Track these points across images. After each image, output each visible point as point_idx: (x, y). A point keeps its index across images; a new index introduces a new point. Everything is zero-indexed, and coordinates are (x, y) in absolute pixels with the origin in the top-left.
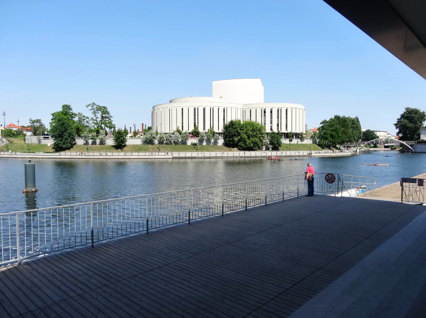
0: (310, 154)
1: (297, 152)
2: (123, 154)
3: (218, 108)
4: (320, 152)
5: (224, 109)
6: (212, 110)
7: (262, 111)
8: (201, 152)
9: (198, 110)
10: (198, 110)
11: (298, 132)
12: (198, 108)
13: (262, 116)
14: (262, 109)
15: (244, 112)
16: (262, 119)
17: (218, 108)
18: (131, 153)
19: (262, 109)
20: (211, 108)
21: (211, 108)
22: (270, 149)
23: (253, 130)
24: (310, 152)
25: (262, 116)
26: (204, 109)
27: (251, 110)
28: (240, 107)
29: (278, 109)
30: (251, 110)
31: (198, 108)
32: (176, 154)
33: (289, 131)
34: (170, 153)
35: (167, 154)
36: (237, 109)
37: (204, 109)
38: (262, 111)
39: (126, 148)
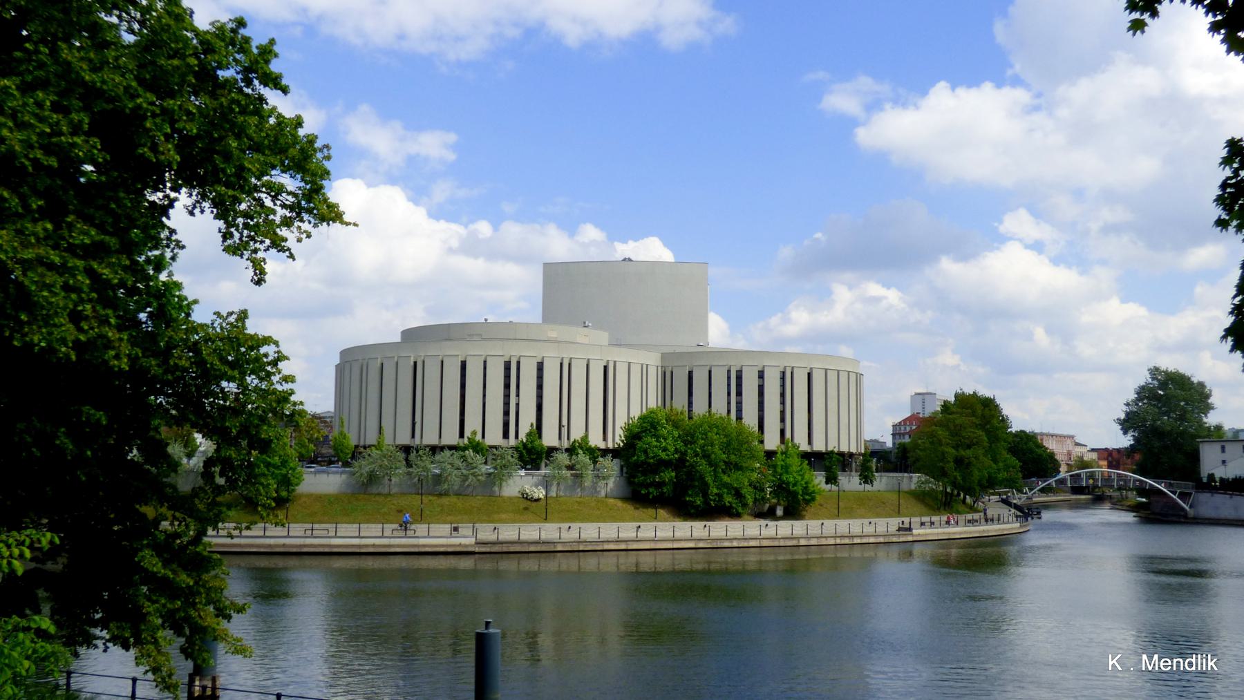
0: (906, 530)
1: (866, 521)
2: (297, 529)
3: (588, 366)
4: (932, 523)
5: (606, 368)
6: (565, 369)
7: (729, 378)
8: (566, 525)
9: (518, 369)
10: (518, 369)
11: (844, 449)
12: (518, 363)
13: (729, 394)
14: (729, 371)
15: (667, 379)
16: (729, 403)
17: (588, 366)
18: (331, 527)
19: (729, 371)
20: (561, 364)
21: (561, 364)
22: (780, 512)
23: (727, 447)
24: (907, 520)
25: (729, 394)
26: (540, 368)
27: (690, 373)
28: (653, 360)
29: (784, 373)
30: (690, 373)
31: (518, 363)
32: (486, 533)
33: (819, 446)
34: (466, 529)
35: (456, 529)
36: (644, 369)
37: (540, 368)
38: (729, 378)
39: (293, 508)
